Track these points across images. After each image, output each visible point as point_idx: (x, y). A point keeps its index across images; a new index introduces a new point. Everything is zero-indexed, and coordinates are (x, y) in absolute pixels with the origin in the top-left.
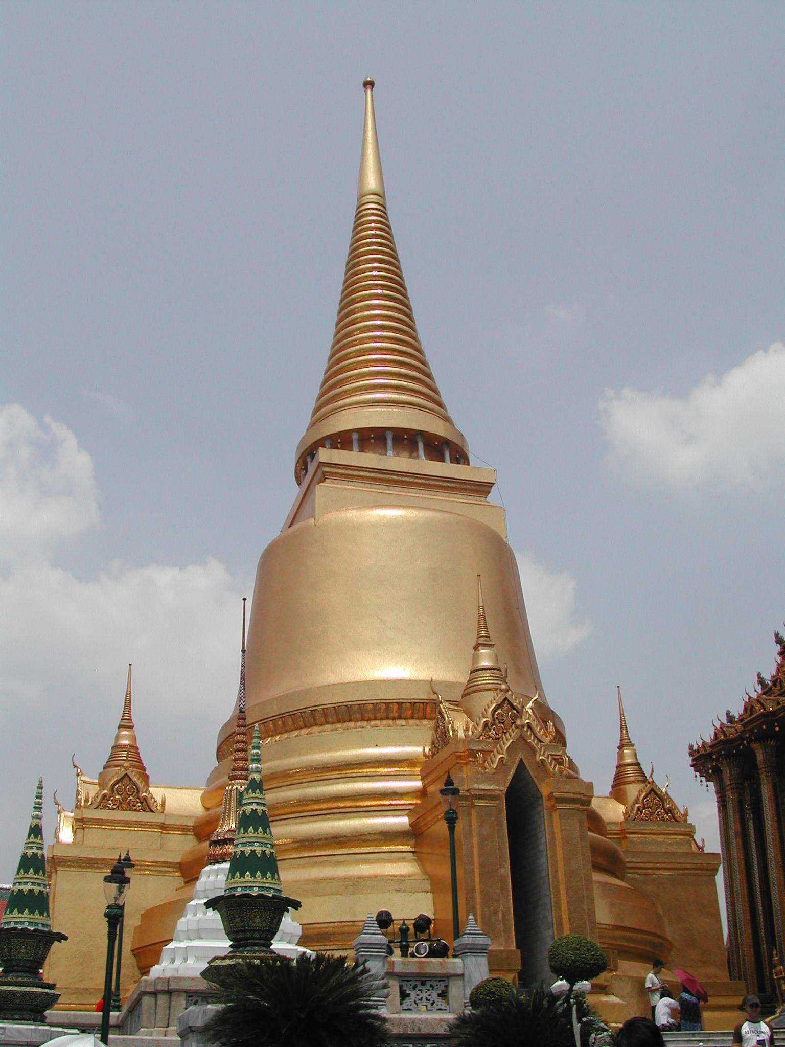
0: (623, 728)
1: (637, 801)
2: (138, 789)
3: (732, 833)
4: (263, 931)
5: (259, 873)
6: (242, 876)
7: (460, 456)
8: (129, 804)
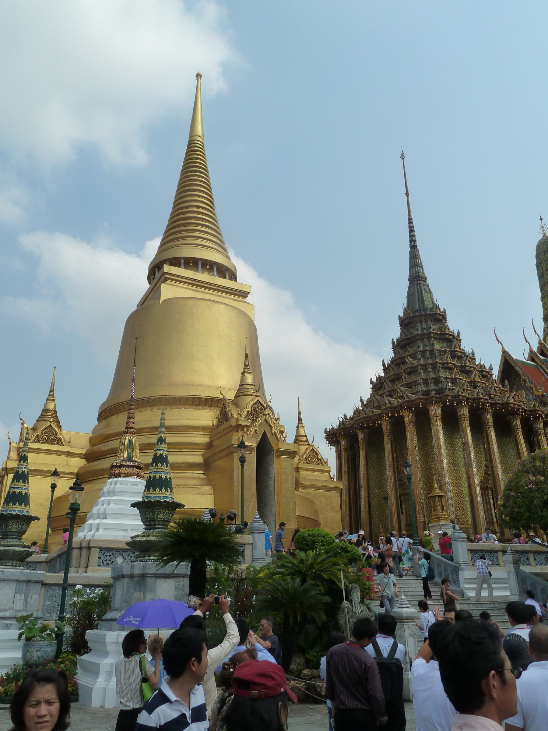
0: (300, 418)
1: (305, 453)
3: (343, 472)
4: (165, 521)
5: (163, 489)
6: (154, 490)
7: (233, 277)
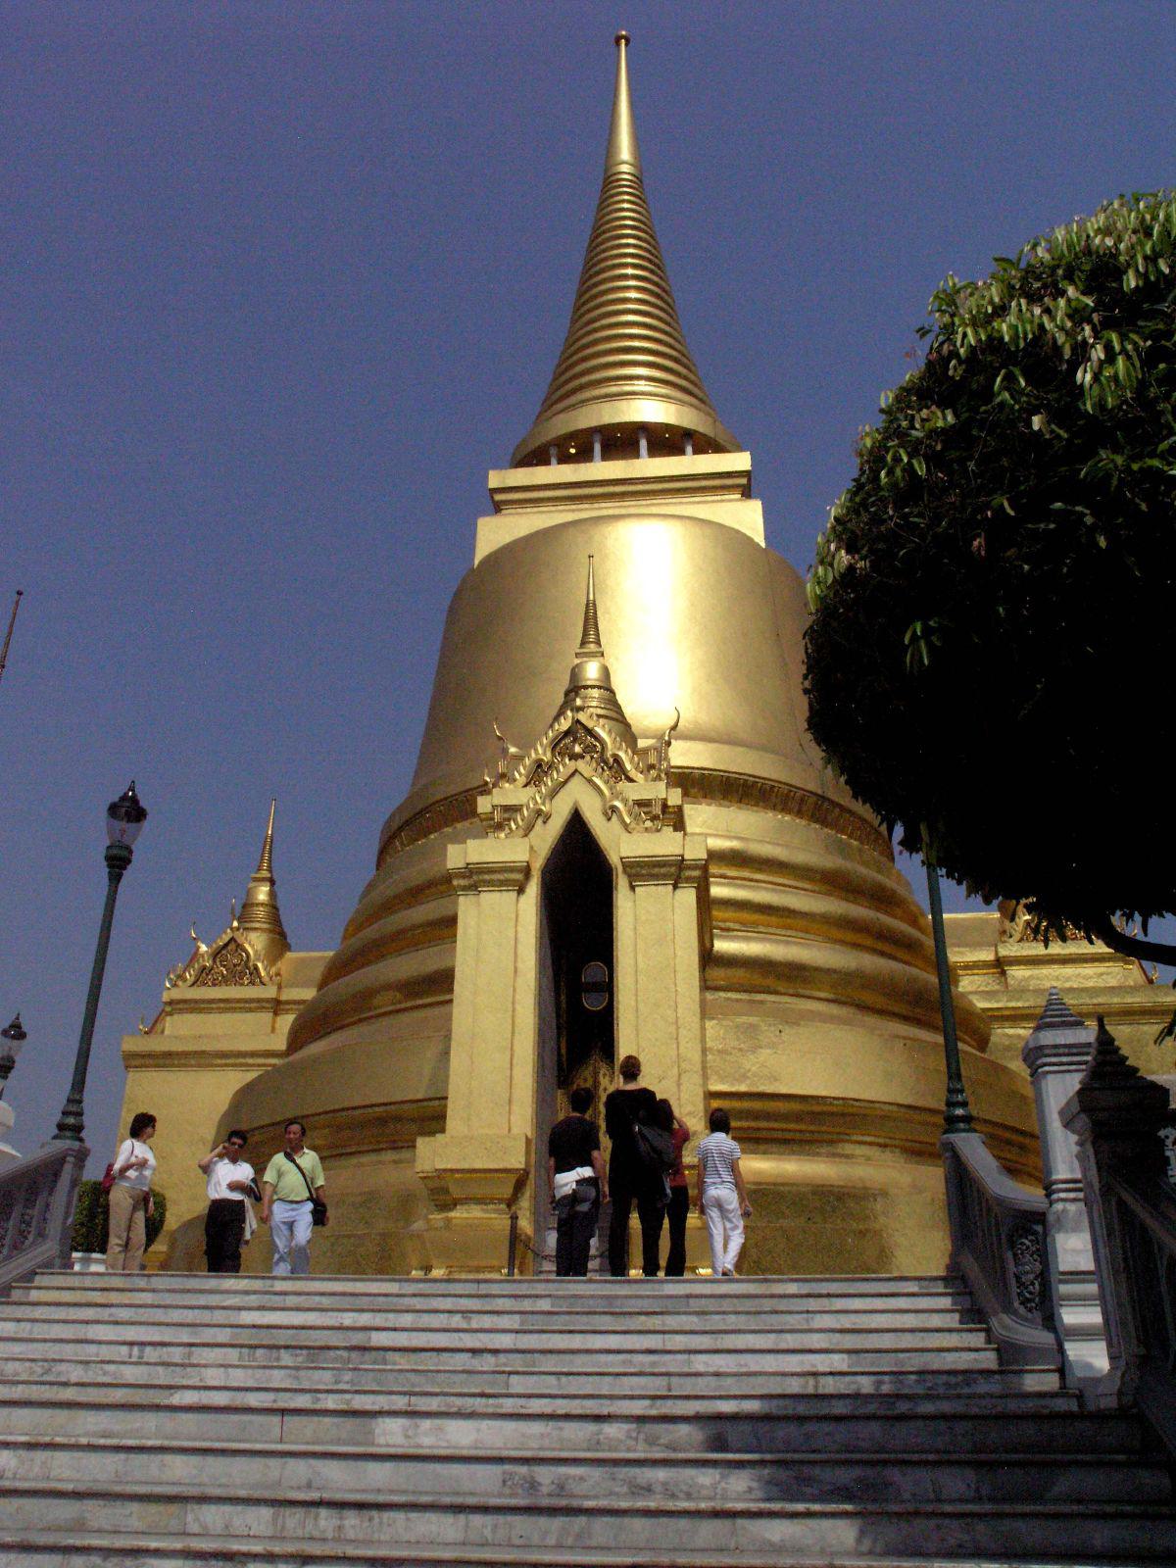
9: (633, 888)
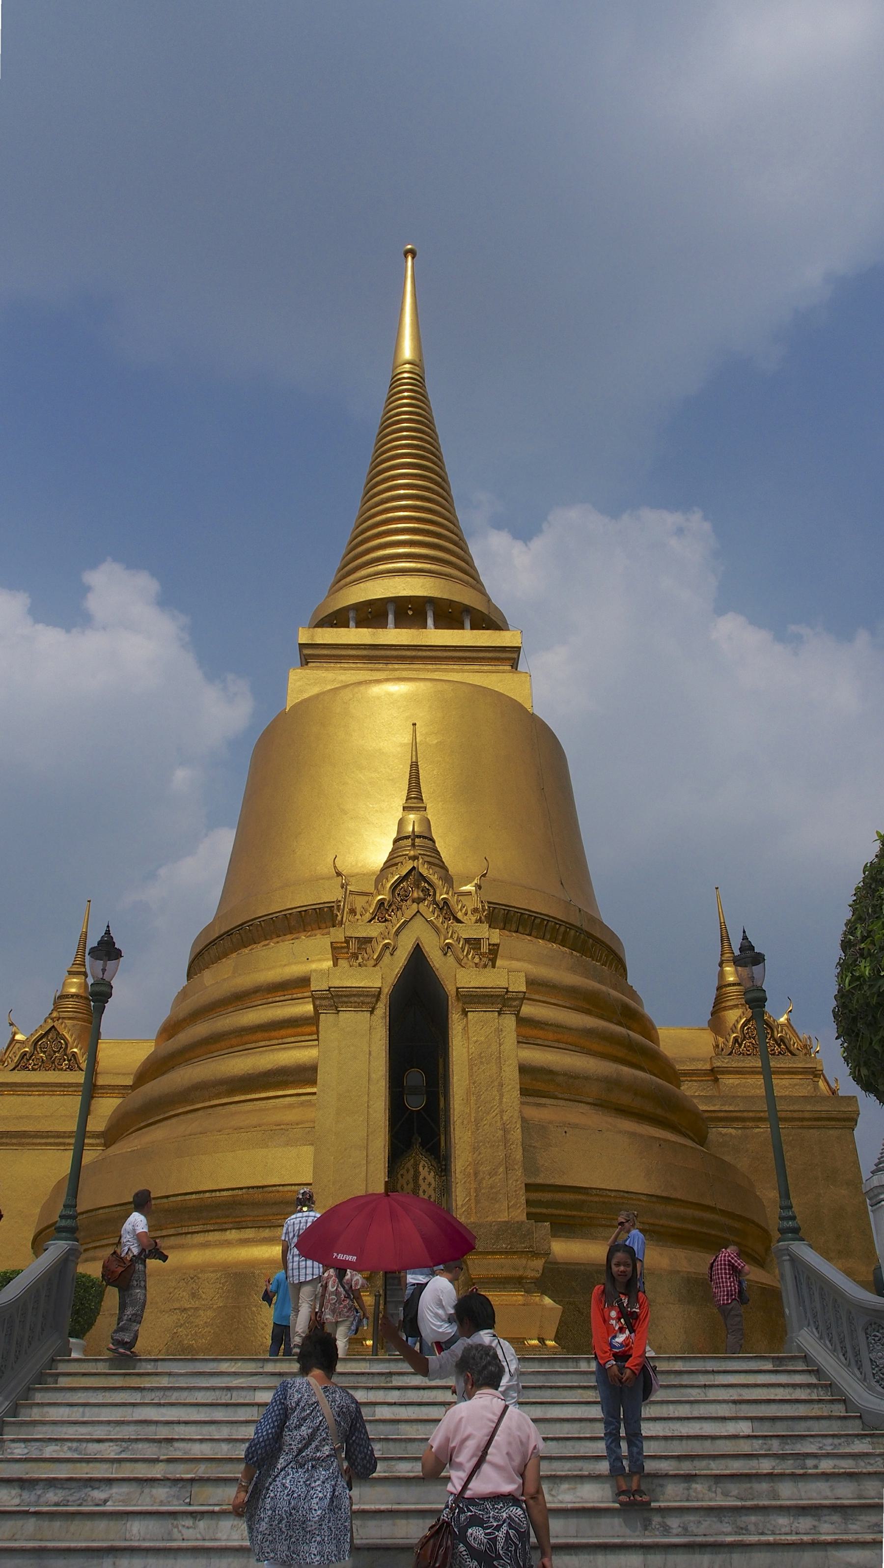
2: (66, 1044)
8: (53, 1062)
9: (465, 1013)
